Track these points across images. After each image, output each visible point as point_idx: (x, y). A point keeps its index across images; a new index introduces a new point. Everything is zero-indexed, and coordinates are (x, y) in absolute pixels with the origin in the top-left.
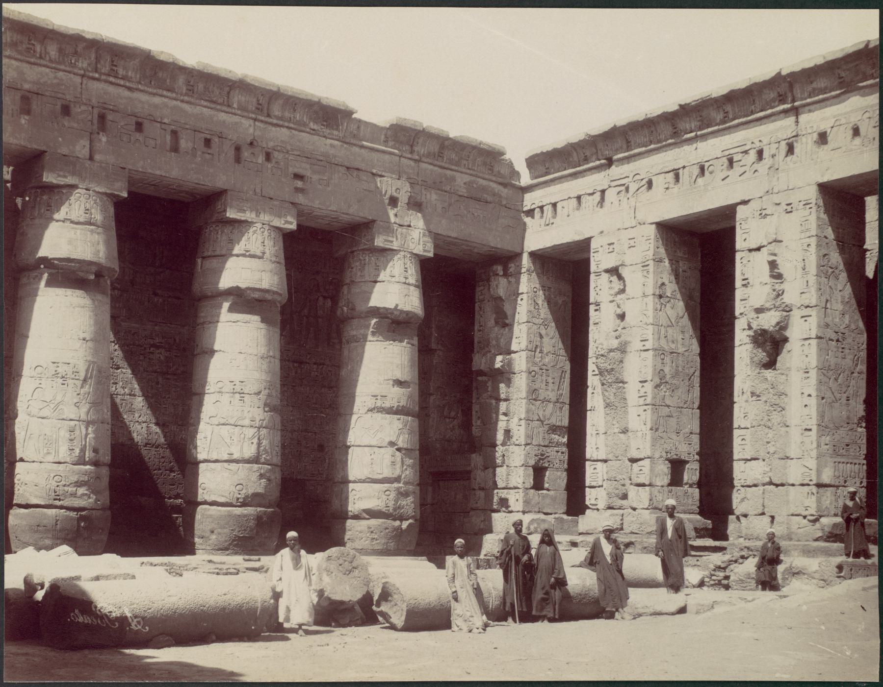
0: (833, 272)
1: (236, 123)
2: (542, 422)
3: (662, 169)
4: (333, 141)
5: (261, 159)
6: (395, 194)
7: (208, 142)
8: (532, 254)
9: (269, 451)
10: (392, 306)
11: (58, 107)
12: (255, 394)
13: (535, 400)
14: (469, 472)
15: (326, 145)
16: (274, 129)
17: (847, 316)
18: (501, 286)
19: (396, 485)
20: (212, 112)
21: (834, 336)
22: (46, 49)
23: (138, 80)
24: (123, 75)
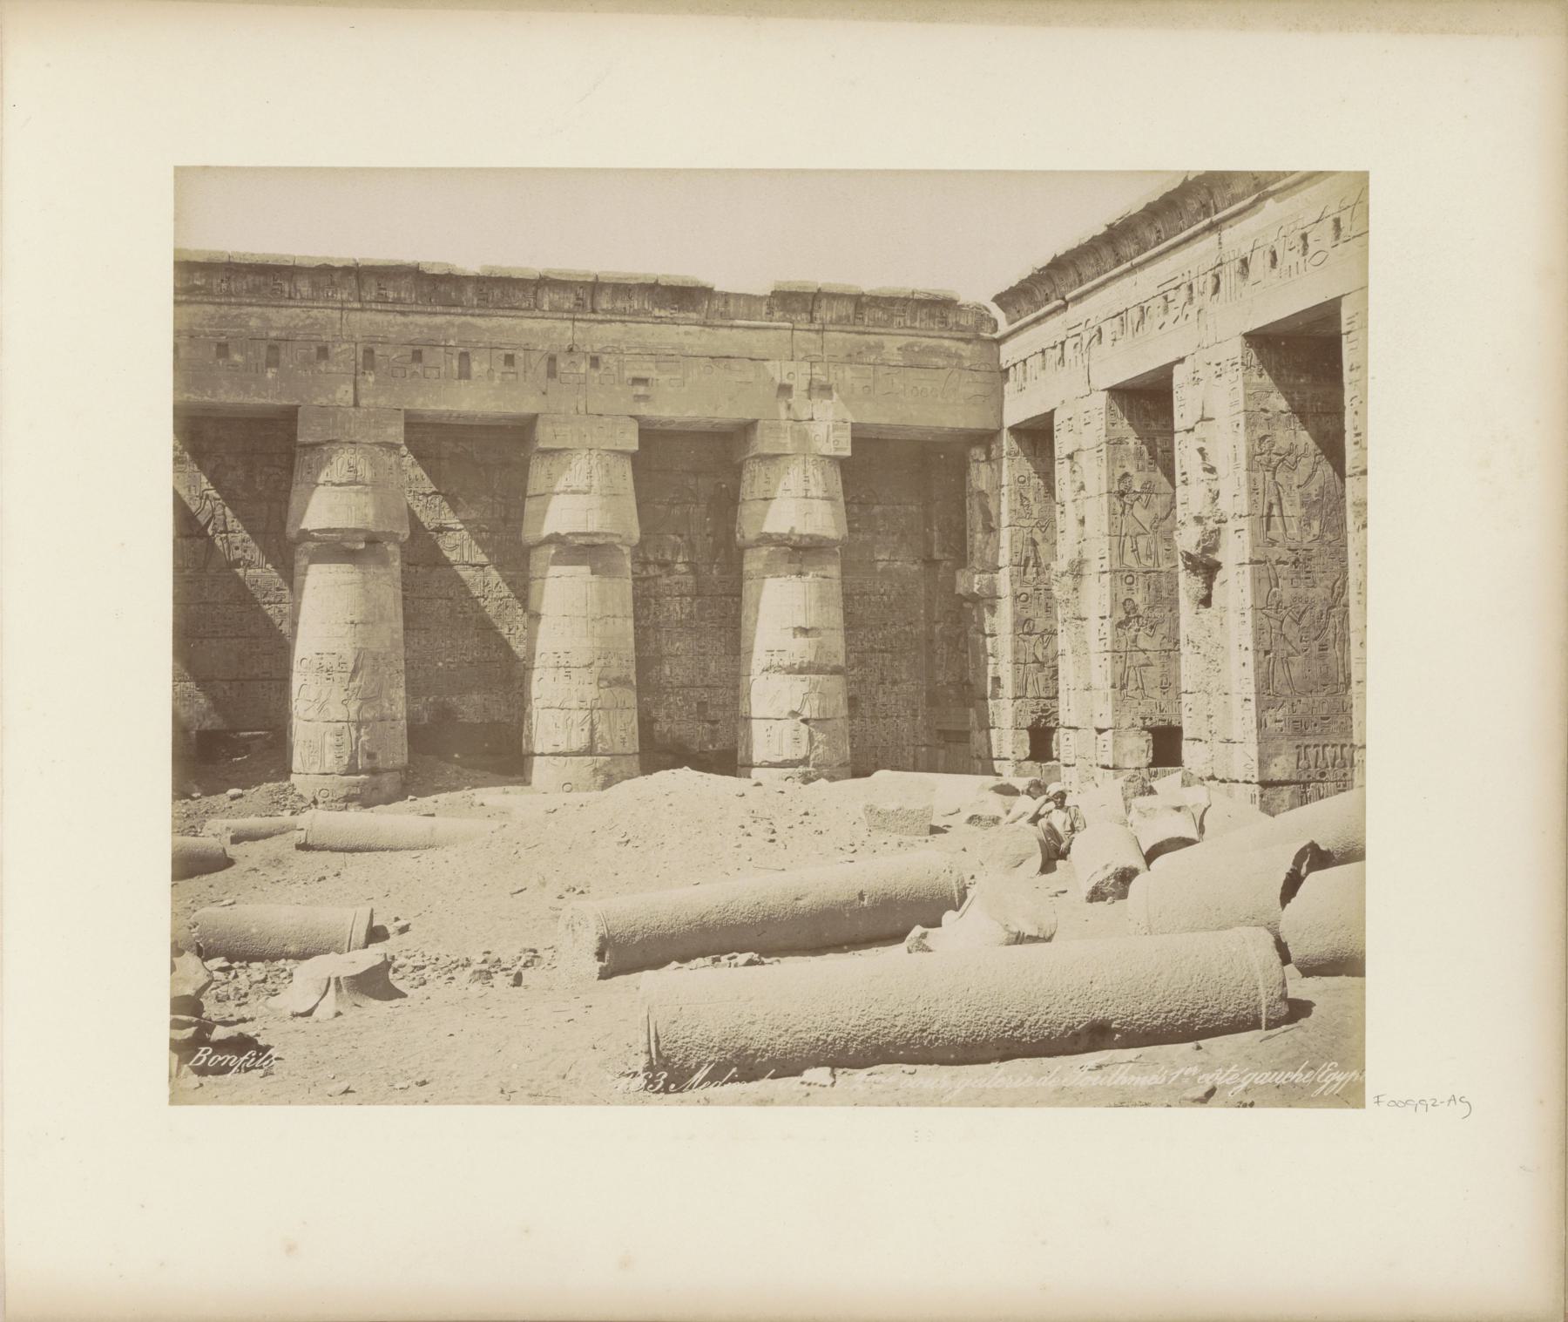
0: (1284, 459)
1: (549, 329)
2: (1042, 664)
3: (1109, 311)
4: (687, 328)
5: (584, 367)
6: (786, 381)
7: (509, 360)
8: (1016, 430)
9: (608, 737)
10: (786, 530)
11: (314, 350)
12: (585, 666)
13: (1029, 634)
14: (968, 733)
15: (678, 333)
16: (601, 326)
17: (1316, 524)
18: (980, 477)
19: (801, 769)
20: (515, 321)
21: (1287, 556)
22: (295, 286)
23: (414, 300)
24: (394, 298)
